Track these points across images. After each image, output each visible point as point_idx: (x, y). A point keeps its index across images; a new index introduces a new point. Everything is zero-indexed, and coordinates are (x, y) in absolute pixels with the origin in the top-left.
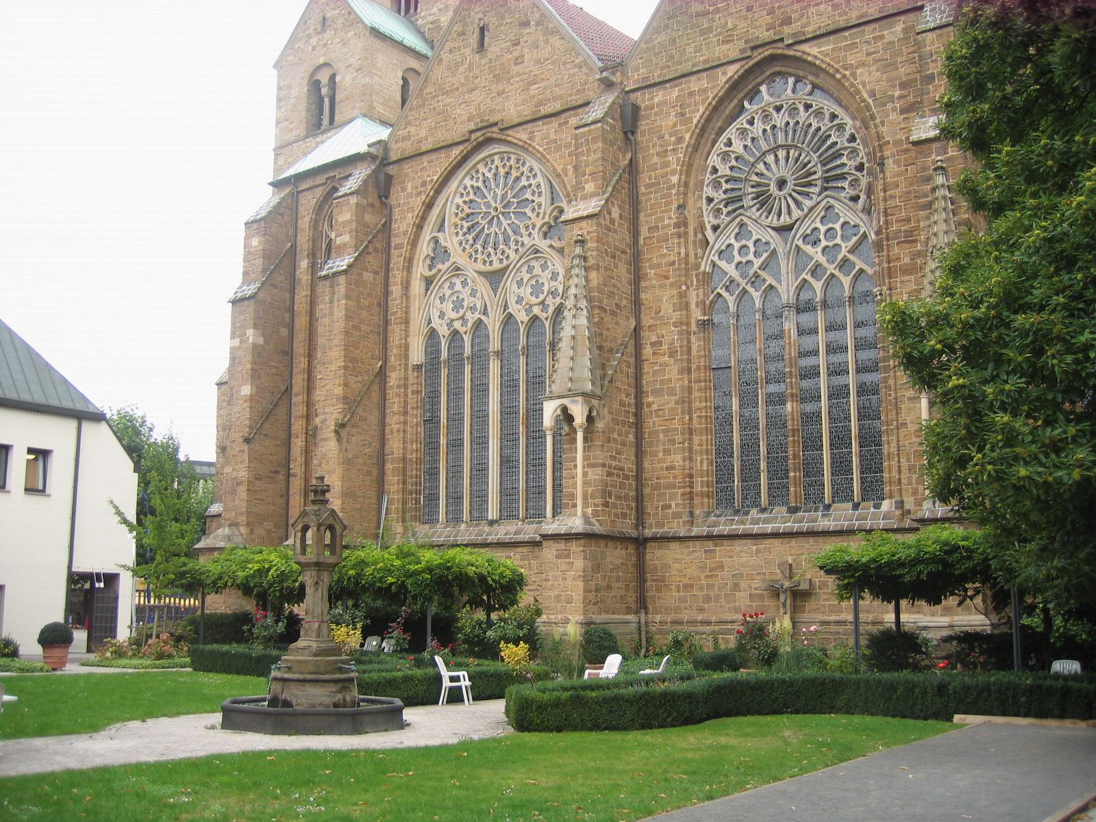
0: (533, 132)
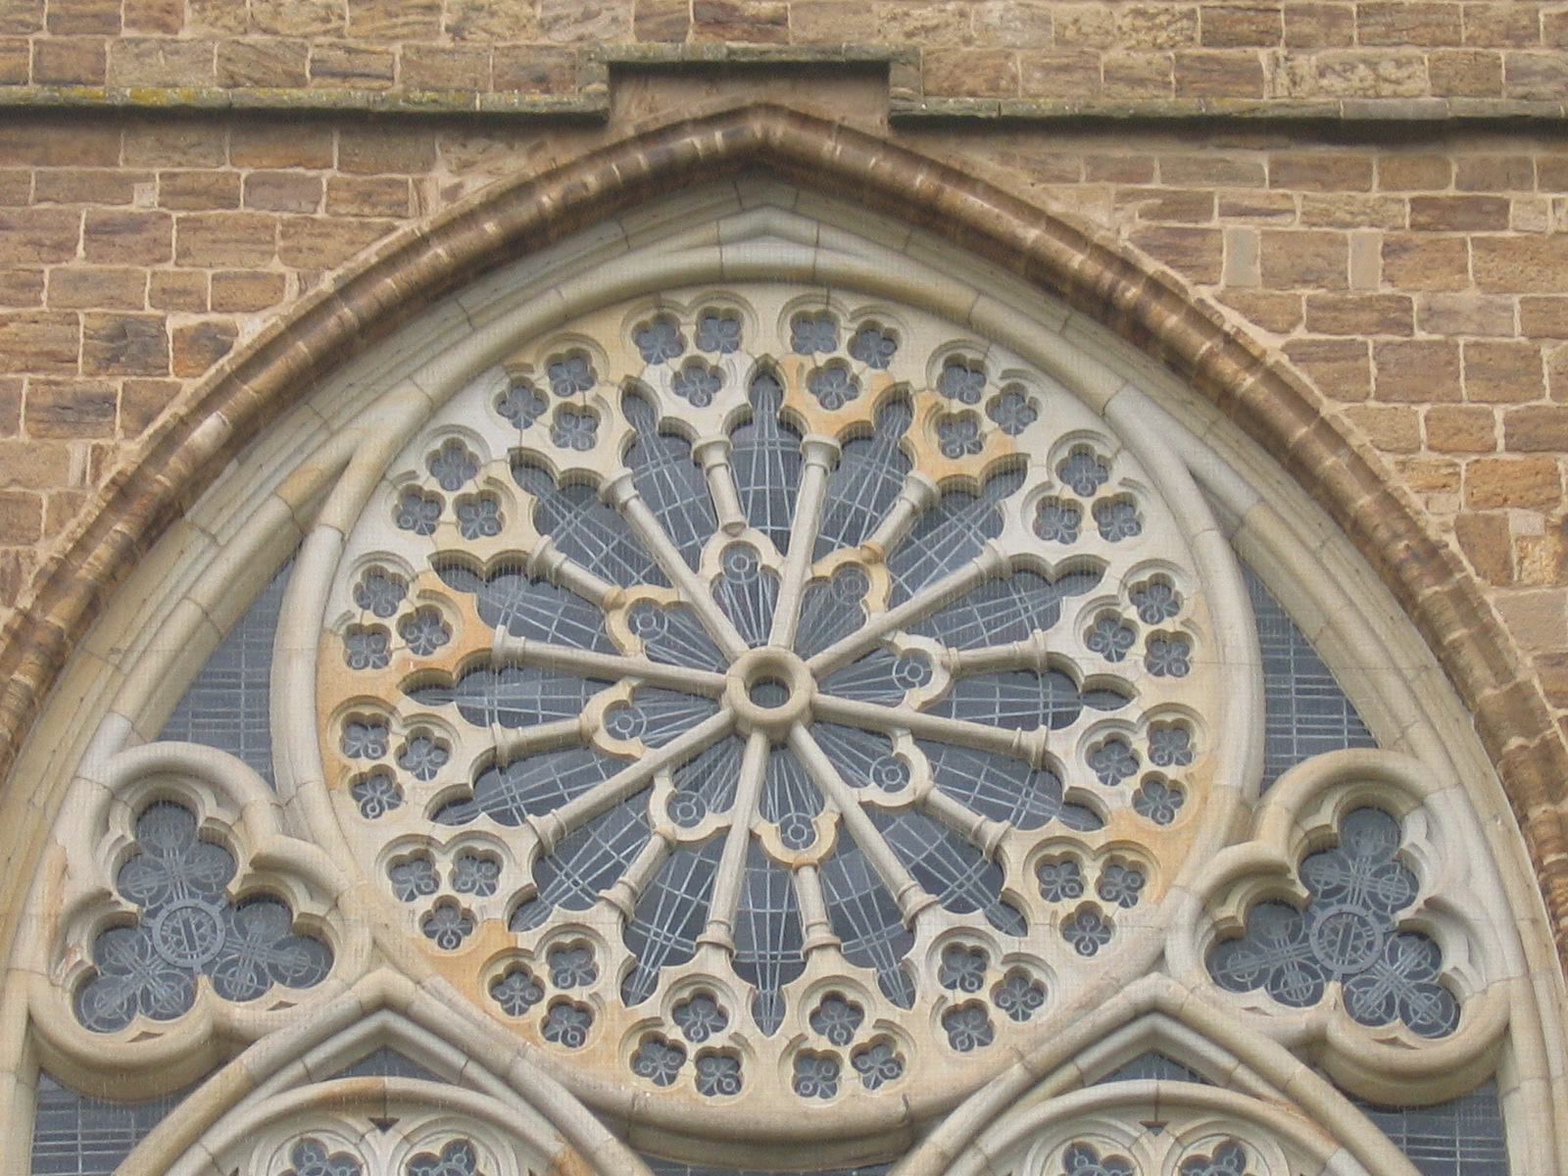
0: (1199, 207)
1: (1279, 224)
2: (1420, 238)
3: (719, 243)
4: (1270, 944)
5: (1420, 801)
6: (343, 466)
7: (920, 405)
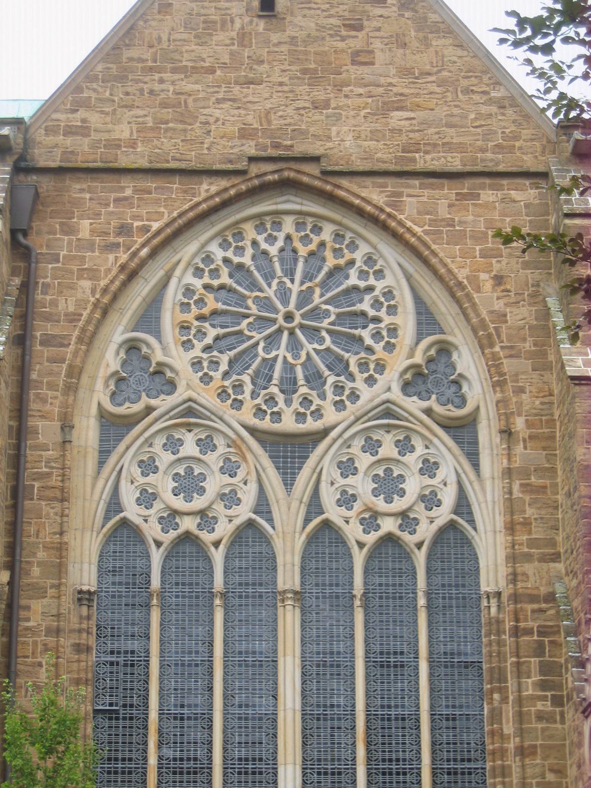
0: (400, 195)
1: (421, 199)
2: (457, 203)
3: (276, 204)
4: (418, 385)
5: (456, 348)
6: (179, 261)
7: (328, 246)
